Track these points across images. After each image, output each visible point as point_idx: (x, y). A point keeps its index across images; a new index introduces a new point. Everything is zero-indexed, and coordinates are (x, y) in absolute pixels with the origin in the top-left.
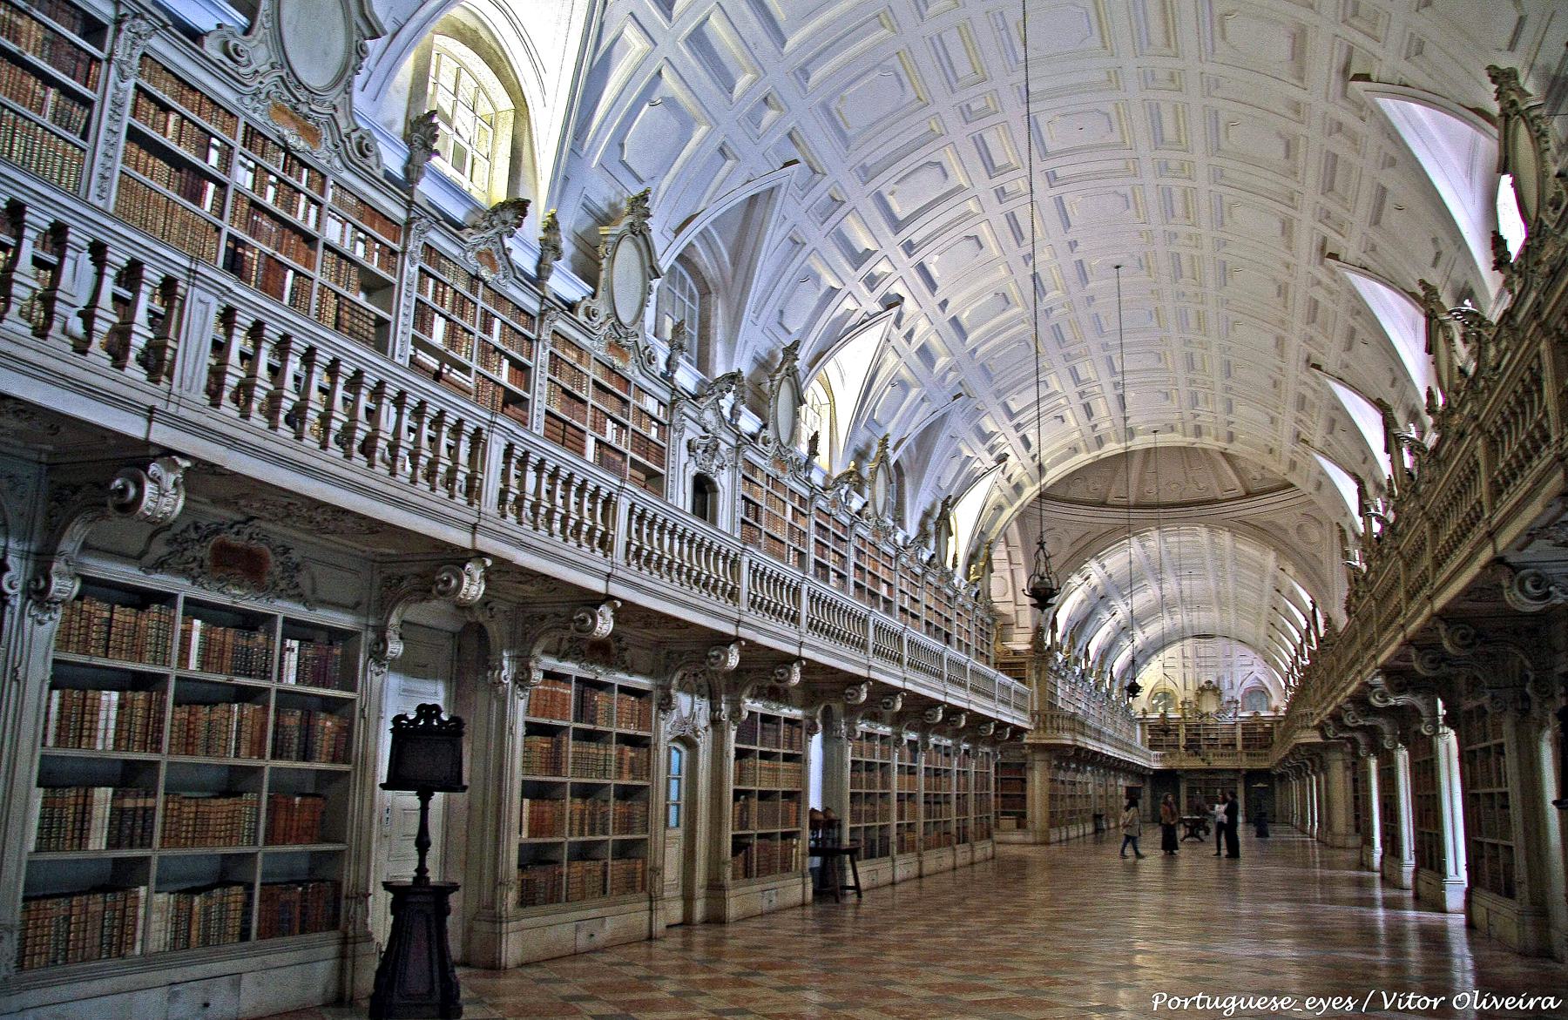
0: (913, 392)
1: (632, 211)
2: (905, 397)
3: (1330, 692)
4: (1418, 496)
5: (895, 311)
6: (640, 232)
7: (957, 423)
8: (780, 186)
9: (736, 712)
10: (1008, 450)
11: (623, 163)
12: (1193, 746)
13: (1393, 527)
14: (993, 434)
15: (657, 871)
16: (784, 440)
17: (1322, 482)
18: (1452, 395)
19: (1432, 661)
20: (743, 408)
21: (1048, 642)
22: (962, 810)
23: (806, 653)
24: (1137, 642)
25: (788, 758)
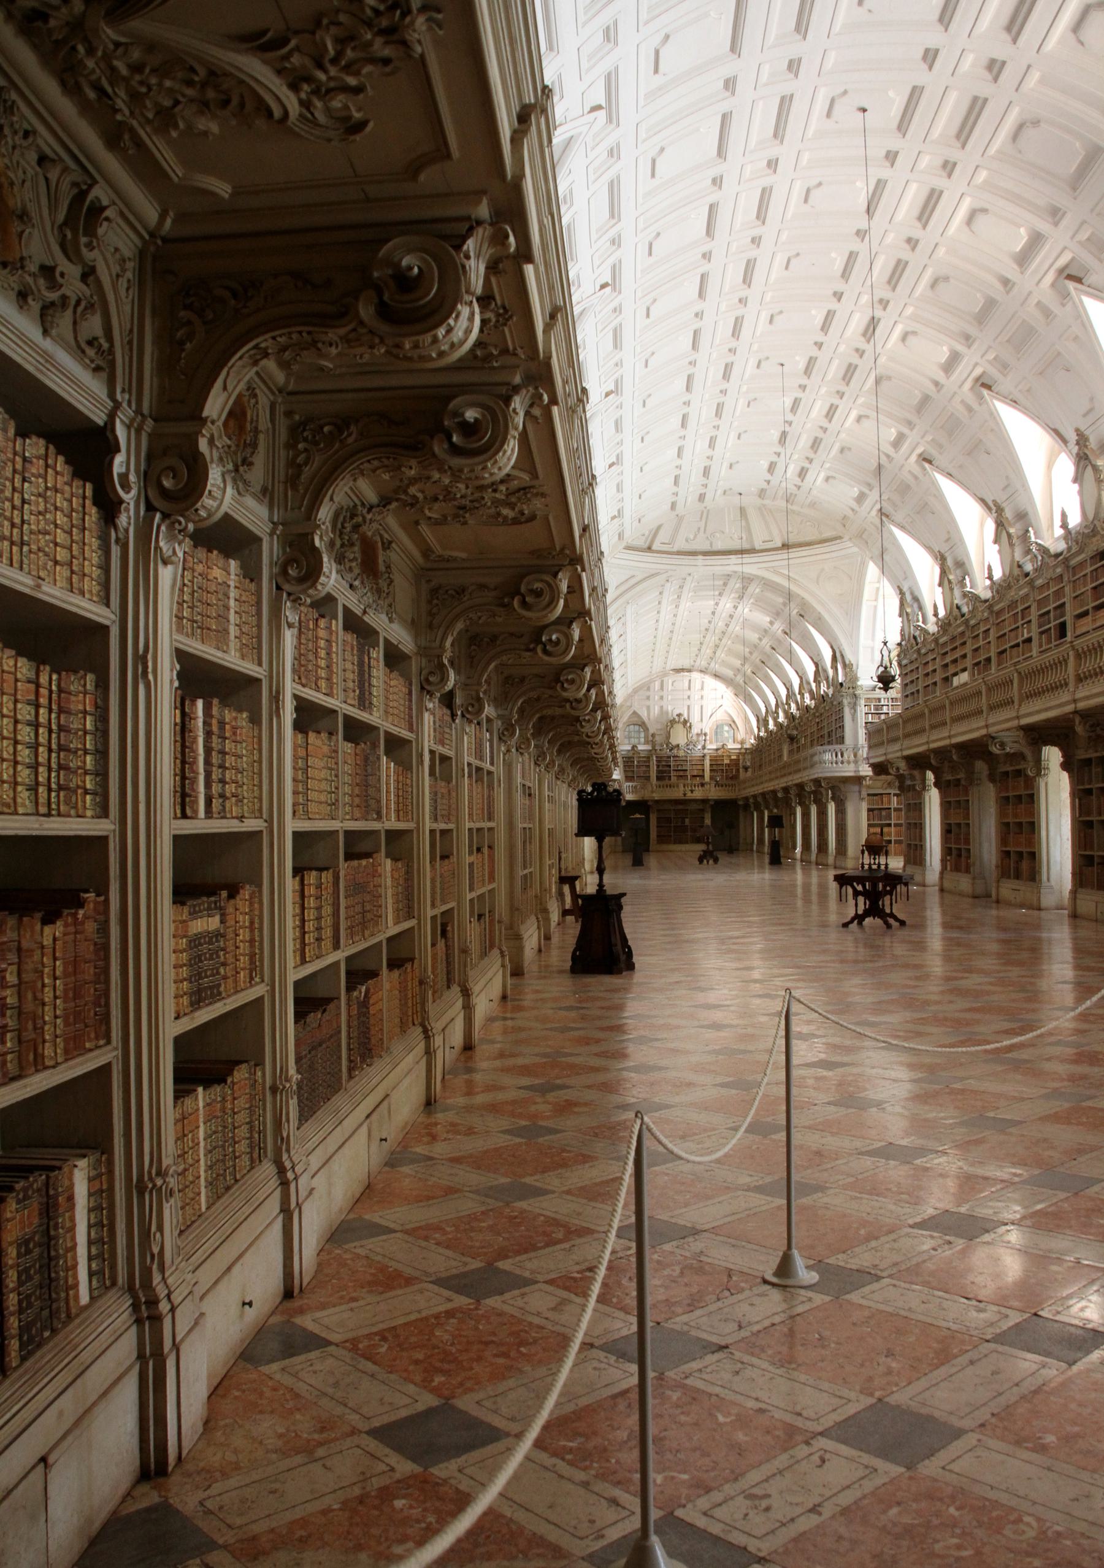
4: (1033, 587)
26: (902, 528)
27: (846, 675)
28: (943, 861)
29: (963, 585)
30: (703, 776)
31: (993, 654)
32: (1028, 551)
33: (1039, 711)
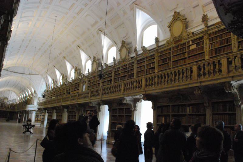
27: (36, 95)
28: (47, 124)
29: (56, 84)
30: (8, 107)
31: (59, 95)
32: (66, 81)
33: (64, 104)
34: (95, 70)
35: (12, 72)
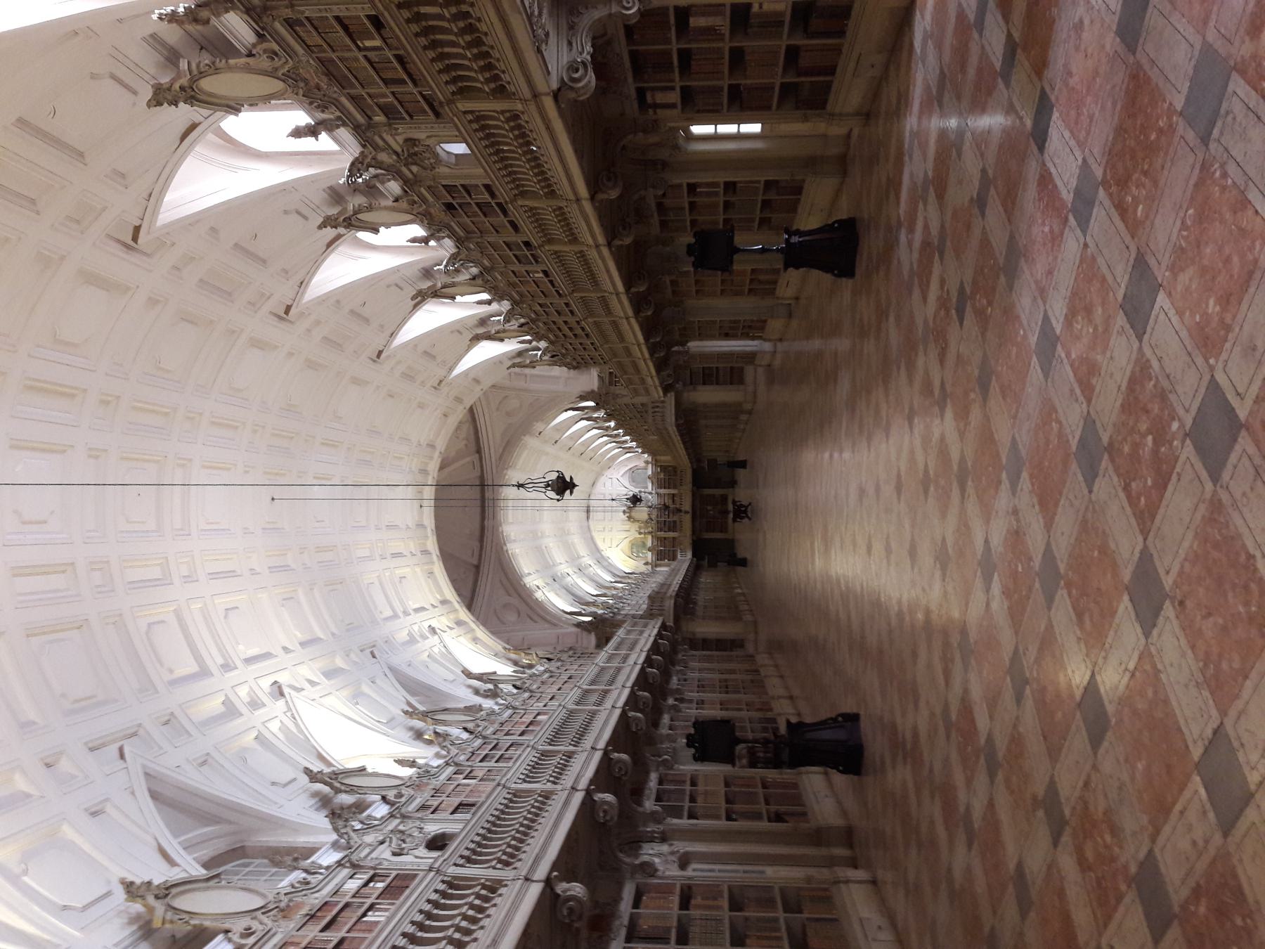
0: (366, 689)
1: (142, 897)
2: (369, 696)
3: (638, 371)
4: (492, 268)
5: (286, 690)
6: (165, 892)
7: (398, 660)
8: (144, 766)
9: (654, 817)
10: (426, 625)
11: (85, 908)
12: (672, 527)
13: (515, 303)
14: (410, 634)
15: (809, 880)
16: (399, 782)
17: (474, 376)
18: (416, 209)
19: (624, 229)
20: (365, 814)
21: (589, 619)
22: (733, 672)
23: (601, 744)
24: (590, 562)
25: (693, 784)
26: (451, 369)
28: (753, 338)
34: (272, 74)
35: (481, 538)
